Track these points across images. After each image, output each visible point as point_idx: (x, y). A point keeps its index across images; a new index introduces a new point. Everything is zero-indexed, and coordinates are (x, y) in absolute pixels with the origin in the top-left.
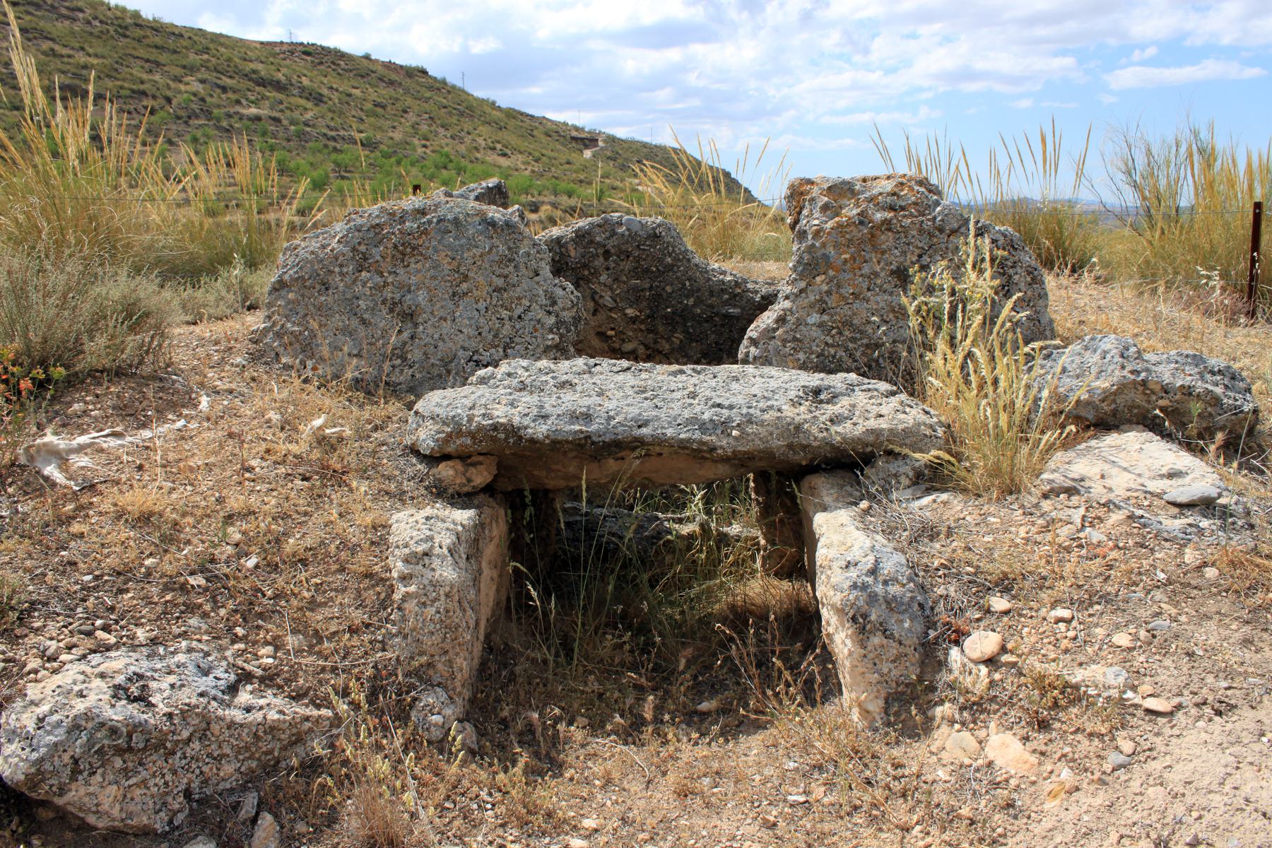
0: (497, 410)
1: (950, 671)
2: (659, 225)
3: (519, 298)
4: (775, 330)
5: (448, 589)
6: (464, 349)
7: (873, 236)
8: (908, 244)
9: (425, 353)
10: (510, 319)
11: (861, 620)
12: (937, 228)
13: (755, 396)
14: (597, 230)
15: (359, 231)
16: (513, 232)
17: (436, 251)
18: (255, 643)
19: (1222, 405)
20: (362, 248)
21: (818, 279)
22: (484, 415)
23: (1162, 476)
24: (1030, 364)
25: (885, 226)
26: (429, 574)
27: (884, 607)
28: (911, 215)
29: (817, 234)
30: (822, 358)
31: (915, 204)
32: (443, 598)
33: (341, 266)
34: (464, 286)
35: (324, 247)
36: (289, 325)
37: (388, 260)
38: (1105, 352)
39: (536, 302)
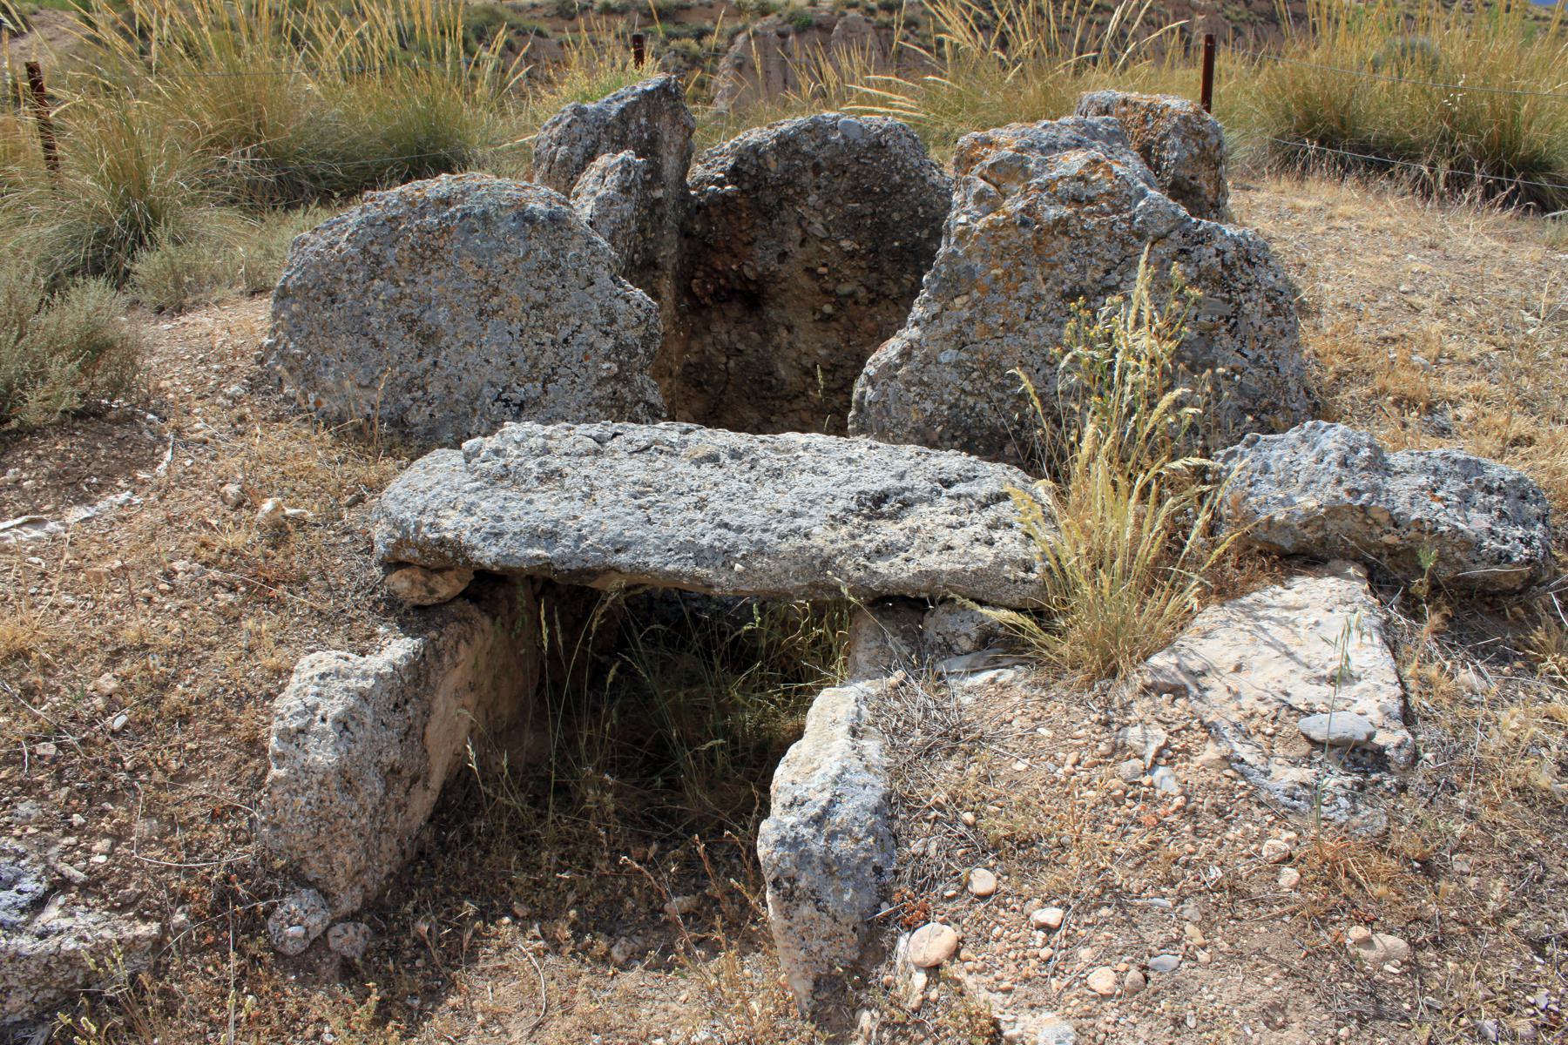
0: (448, 518)
1: (892, 966)
2: (886, 131)
3: (565, 316)
5: (320, 777)
6: (493, 385)
7: (1040, 242)
8: (1090, 255)
9: (447, 387)
10: (553, 343)
11: (787, 885)
12: (1134, 233)
13: (779, 511)
14: (804, 136)
15: (372, 226)
16: (560, 229)
18: (92, 834)
19: (1481, 548)
20: (375, 249)
21: (958, 301)
22: (431, 525)
23: (1320, 679)
24: (1230, 449)
25: (1060, 228)
26: (301, 757)
27: (819, 871)
28: (1102, 213)
29: (962, 236)
30: (955, 410)
31: (1110, 194)
32: (316, 787)
33: (350, 272)
34: (495, 301)
35: (331, 245)
36: (291, 345)
37: (405, 265)
38: (1324, 453)
39: (588, 320)
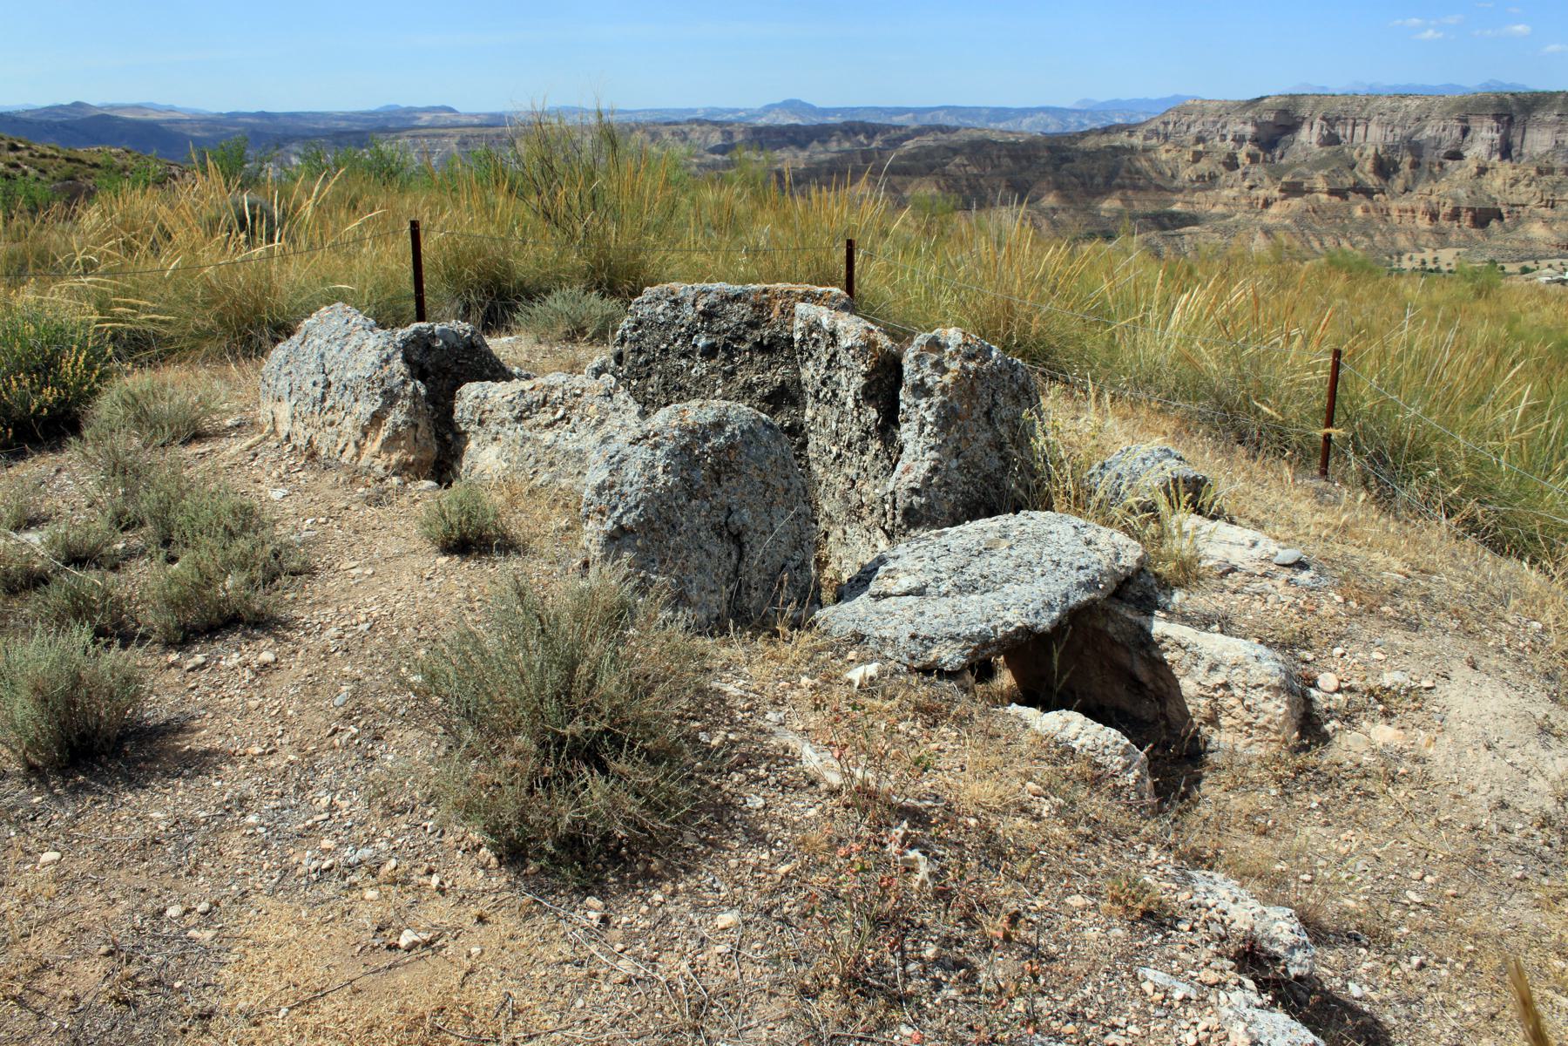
4: (930, 479)
17: (747, 465)
29: (944, 390)
